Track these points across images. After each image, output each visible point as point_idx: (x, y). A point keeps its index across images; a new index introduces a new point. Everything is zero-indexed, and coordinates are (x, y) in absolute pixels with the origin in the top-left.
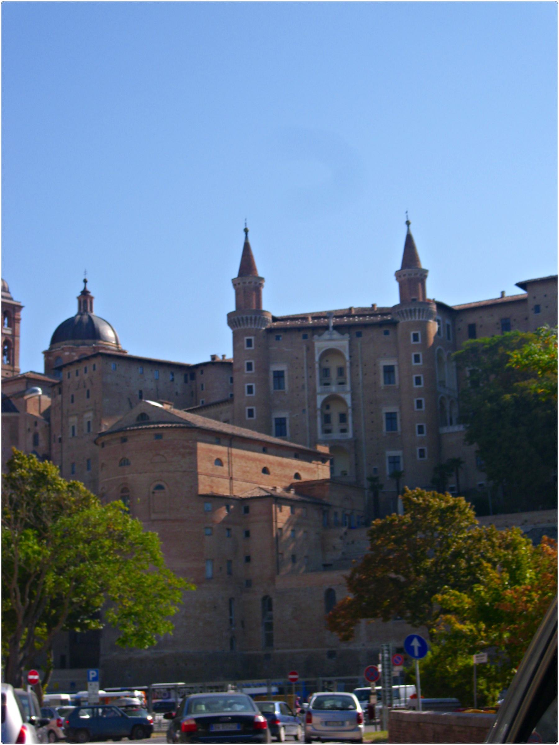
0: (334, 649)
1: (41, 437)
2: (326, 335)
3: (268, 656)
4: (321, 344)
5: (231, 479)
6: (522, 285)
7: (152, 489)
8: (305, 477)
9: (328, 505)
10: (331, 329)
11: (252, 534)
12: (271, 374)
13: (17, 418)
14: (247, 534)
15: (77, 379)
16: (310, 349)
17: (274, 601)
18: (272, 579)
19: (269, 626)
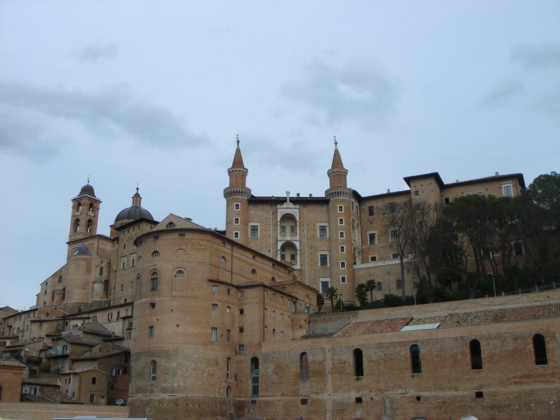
0: (306, 398)
1: (104, 270)
2: (285, 205)
3: (254, 402)
4: (282, 210)
5: (232, 272)
6: (408, 180)
7: (174, 273)
8: (278, 280)
9: (297, 299)
10: (288, 201)
11: (245, 311)
12: (250, 227)
13: (91, 259)
14: (242, 312)
15: (128, 235)
16: (275, 213)
17: (260, 361)
18: (260, 345)
19: (256, 380)
